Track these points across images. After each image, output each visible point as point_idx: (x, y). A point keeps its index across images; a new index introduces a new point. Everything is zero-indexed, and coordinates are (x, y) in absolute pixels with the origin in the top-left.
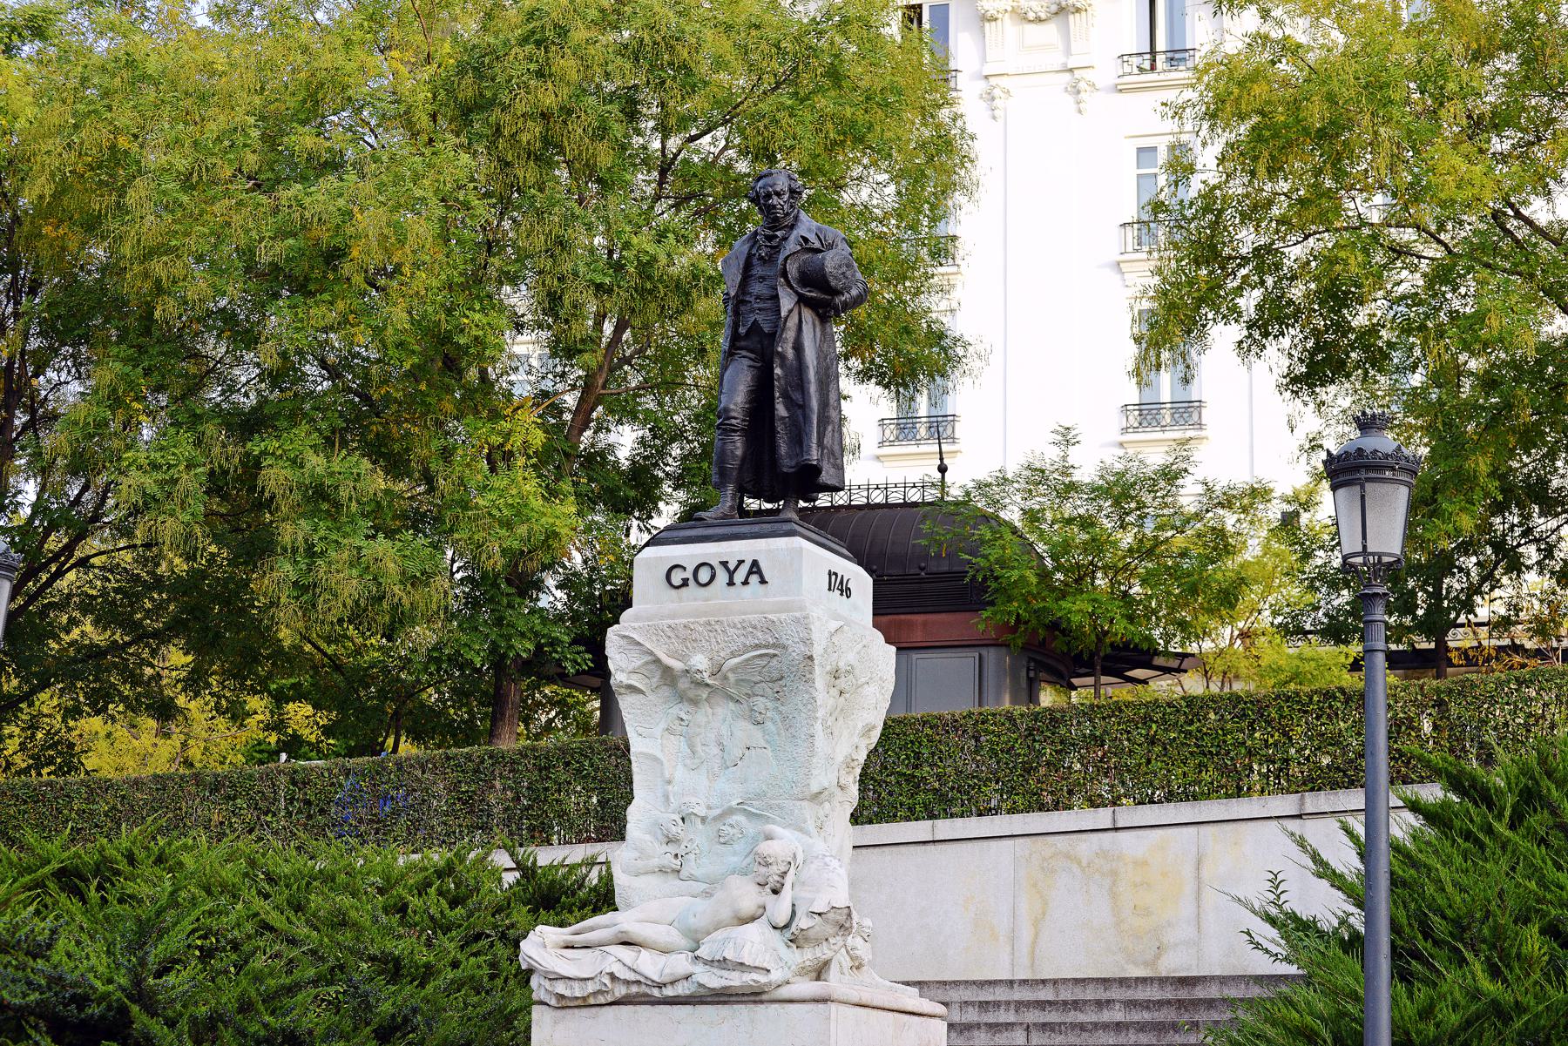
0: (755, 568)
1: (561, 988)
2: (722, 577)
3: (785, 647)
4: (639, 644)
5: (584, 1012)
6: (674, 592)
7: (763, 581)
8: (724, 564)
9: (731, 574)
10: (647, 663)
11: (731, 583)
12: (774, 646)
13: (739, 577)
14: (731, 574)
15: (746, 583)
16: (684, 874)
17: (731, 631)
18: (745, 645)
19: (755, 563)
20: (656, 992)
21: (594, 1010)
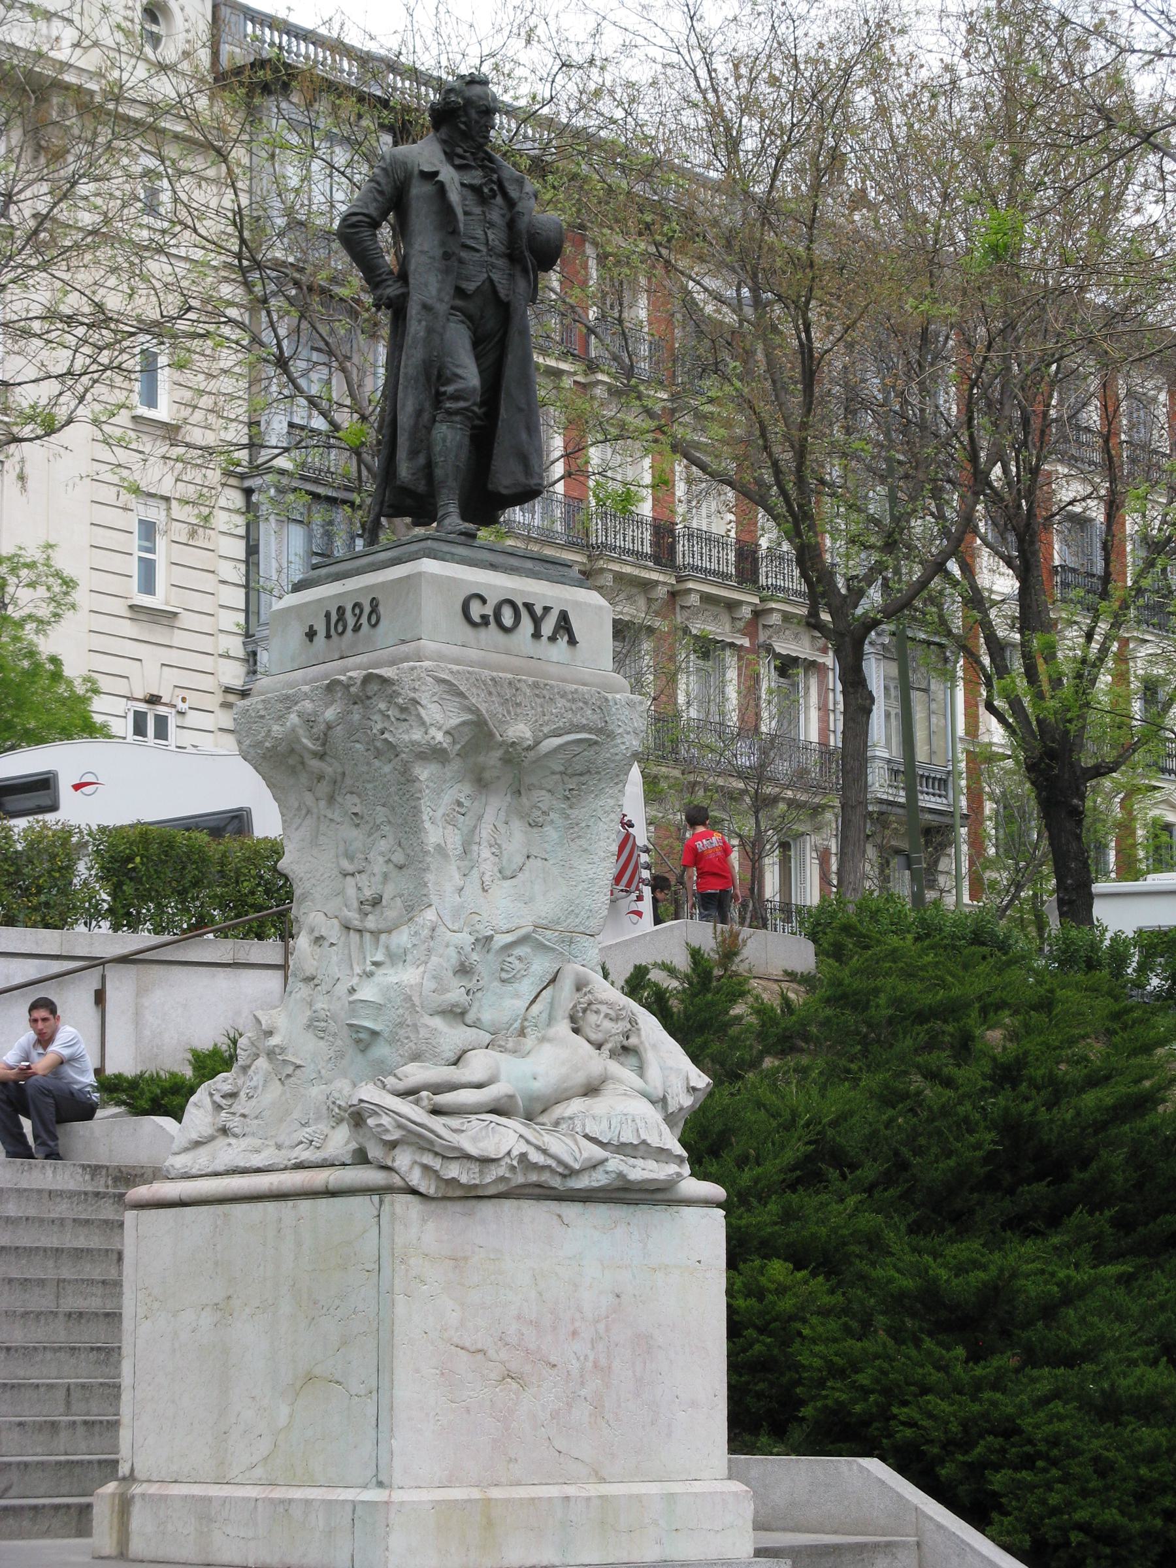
0: (564, 624)
1: (453, 1171)
2: (527, 624)
3: (611, 735)
4: (461, 695)
5: (458, 1207)
6: (468, 629)
7: (572, 641)
8: (529, 607)
9: (537, 622)
10: (464, 723)
11: (537, 635)
12: (599, 731)
13: (548, 628)
14: (537, 622)
15: (553, 639)
16: (470, 1018)
17: (561, 702)
18: (572, 724)
19: (564, 617)
20: (556, 1182)
21: (474, 1202)
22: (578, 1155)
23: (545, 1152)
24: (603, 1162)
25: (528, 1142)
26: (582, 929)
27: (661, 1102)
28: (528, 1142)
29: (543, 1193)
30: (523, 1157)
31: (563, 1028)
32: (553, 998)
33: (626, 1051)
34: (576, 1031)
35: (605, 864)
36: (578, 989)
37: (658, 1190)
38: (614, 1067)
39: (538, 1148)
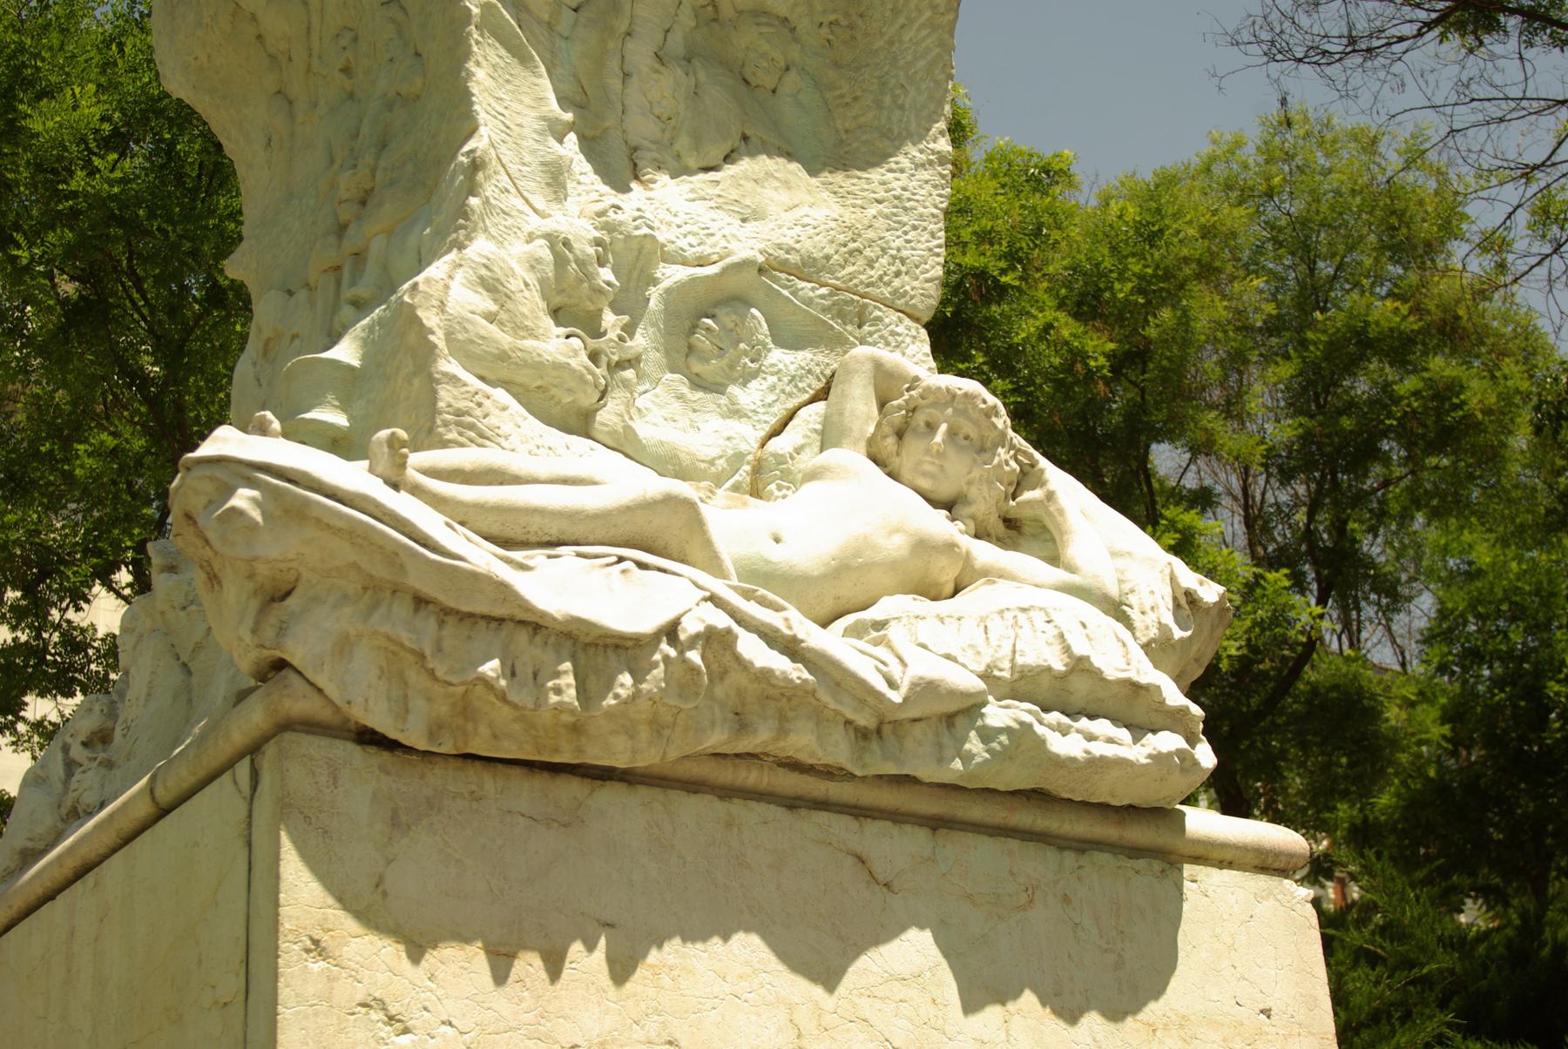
22: (895, 669)
23: (791, 648)
24: (971, 708)
25: (733, 613)
26: (886, 292)
27: (1117, 609)
28: (733, 613)
29: (806, 792)
30: (713, 640)
31: (851, 458)
32: (826, 420)
33: (1013, 529)
34: (892, 475)
35: (924, 175)
36: (882, 404)
37: (1131, 812)
38: (985, 553)
39: (771, 638)
